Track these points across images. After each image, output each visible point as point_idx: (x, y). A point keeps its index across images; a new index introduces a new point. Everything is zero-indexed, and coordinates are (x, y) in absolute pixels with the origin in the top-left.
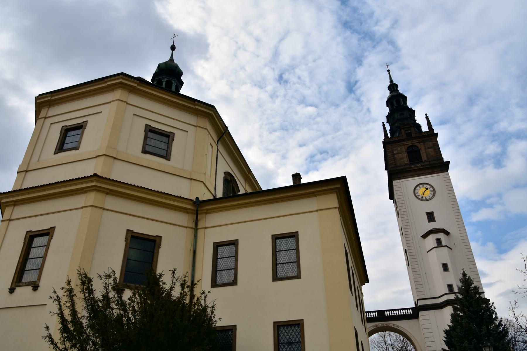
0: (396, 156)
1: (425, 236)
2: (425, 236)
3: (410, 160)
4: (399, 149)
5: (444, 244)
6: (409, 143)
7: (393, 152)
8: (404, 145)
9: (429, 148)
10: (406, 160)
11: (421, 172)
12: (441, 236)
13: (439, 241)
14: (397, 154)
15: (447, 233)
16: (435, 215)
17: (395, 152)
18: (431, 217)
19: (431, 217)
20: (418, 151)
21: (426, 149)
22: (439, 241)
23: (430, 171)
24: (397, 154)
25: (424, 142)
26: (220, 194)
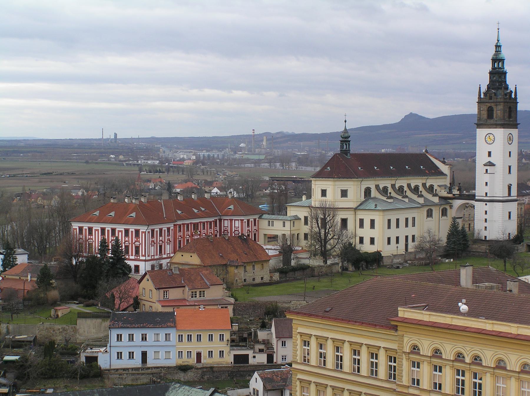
0: (481, 112)
1: (485, 165)
2: (485, 165)
3: (488, 117)
4: (484, 107)
7: (480, 109)
8: (487, 106)
9: (498, 110)
11: (491, 126)
13: (487, 170)
14: (482, 110)
15: (494, 165)
17: (482, 109)
18: (490, 154)
19: (490, 154)
20: (493, 110)
21: (496, 111)
22: (487, 170)
23: (495, 126)
24: (482, 110)
25: (496, 105)
26: (363, 199)
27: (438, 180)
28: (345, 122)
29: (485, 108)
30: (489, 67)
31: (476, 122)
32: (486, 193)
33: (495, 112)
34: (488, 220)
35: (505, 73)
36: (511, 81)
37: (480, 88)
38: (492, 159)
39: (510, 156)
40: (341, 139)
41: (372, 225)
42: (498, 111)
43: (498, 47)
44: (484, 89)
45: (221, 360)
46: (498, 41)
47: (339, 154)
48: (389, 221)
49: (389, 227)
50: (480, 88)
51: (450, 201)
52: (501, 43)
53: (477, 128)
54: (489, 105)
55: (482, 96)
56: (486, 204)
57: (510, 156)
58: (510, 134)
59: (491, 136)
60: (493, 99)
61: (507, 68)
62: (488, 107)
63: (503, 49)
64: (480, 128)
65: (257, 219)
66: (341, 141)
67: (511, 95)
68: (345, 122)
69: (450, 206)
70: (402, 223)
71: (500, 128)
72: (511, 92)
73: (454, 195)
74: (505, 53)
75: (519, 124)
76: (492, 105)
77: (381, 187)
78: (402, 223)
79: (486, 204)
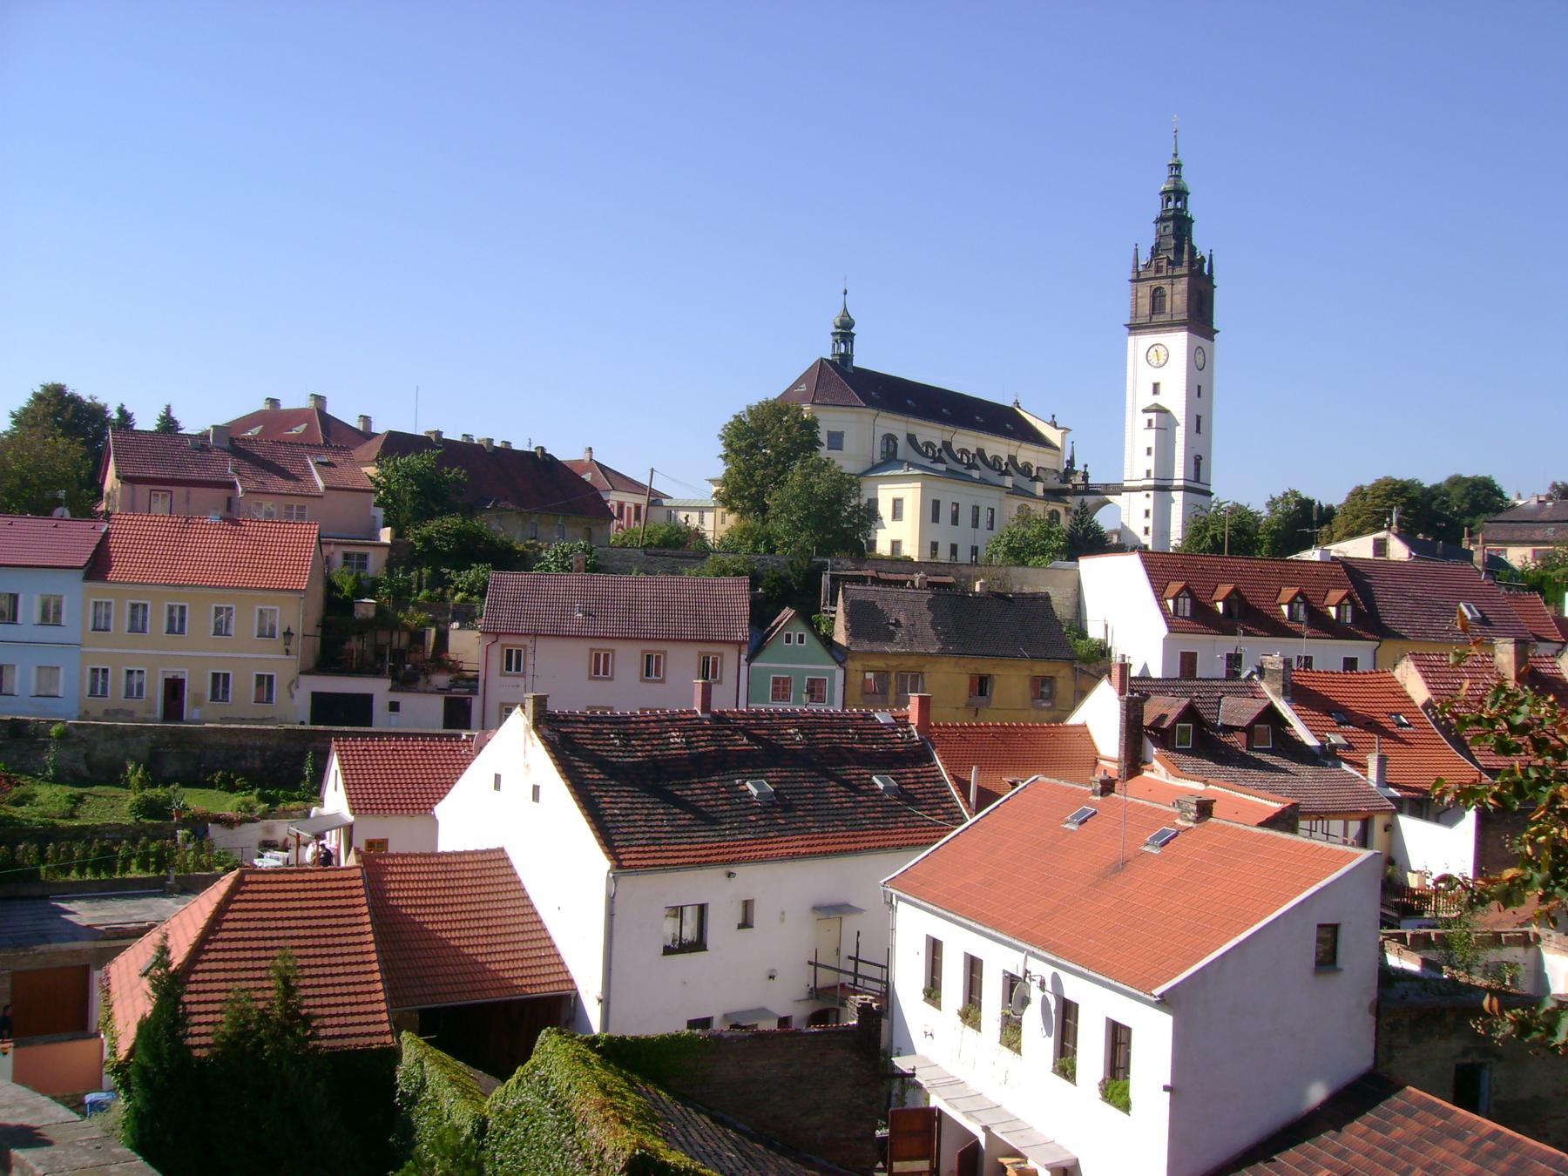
1: (1145, 411)
2: (1145, 411)
5: (1154, 426)
6: (1156, 283)
10: (1145, 307)
12: (1153, 416)
16: (1162, 388)
17: (1139, 295)
18: (1156, 388)
19: (1156, 388)
22: (1150, 422)
26: (878, 459)
27: (1041, 456)
28: (845, 293)
29: (1145, 290)
30: (1155, 208)
32: (1148, 472)
33: (1168, 298)
34: (1151, 530)
35: (1191, 221)
36: (1202, 240)
38: (1162, 400)
39: (1199, 395)
40: (835, 330)
41: (897, 514)
42: (1178, 294)
45: (263, 710)
46: (1175, 155)
47: (827, 360)
48: (936, 504)
49: (936, 518)
51: (1069, 499)
52: (1181, 158)
53: (1130, 334)
54: (1156, 283)
55: (1140, 269)
56: (1148, 496)
57: (1199, 395)
58: (1199, 347)
59: (1161, 349)
60: (1164, 271)
61: (1193, 210)
63: (1184, 171)
64: (1135, 334)
65: (644, 508)
66: (833, 334)
67: (1201, 267)
68: (845, 293)
69: (1066, 508)
70: (965, 517)
71: (1181, 330)
73: (1075, 486)
74: (1188, 180)
75: (1217, 332)
76: (1163, 281)
77: (920, 440)
78: (965, 517)
79: (1148, 496)
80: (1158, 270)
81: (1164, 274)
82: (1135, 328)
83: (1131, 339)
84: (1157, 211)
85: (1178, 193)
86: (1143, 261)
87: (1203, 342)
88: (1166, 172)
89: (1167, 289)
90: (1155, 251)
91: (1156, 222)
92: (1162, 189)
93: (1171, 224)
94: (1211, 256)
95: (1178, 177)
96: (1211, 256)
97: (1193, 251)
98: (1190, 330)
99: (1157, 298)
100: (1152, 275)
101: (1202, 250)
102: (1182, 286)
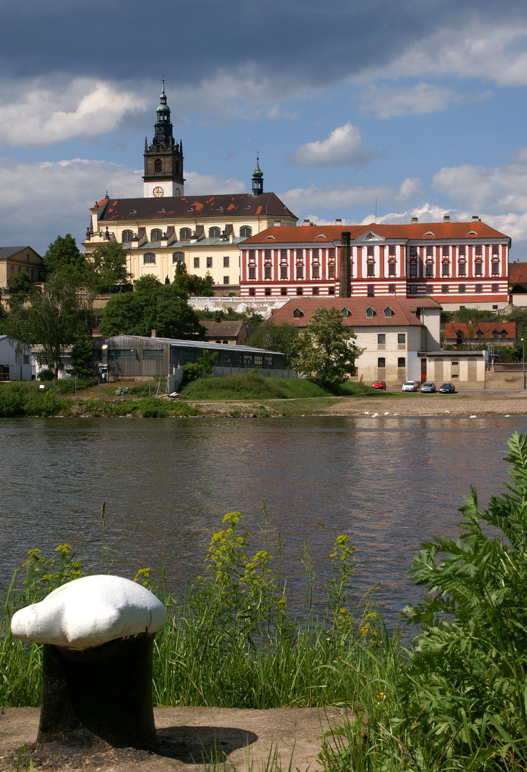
6: (156, 158)
29: (151, 162)
30: (155, 119)
31: (144, 176)
35: (171, 126)
36: (177, 135)
37: (146, 140)
43: (165, 98)
44: (150, 143)
46: (163, 93)
50: (146, 140)
53: (145, 182)
58: (178, 188)
59: (160, 190)
61: (172, 121)
62: (155, 160)
64: (147, 182)
67: (177, 149)
72: (178, 145)
80: (158, 151)
81: (160, 153)
82: (147, 179)
83: (146, 184)
84: (155, 121)
85: (166, 112)
86: (149, 145)
87: (178, 185)
88: (160, 101)
89: (162, 160)
90: (155, 141)
91: (155, 126)
92: (158, 109)
93: (163, 128)
94: (181, 143)
95: (165, 104)
96: (181, 143)
97: (173, 140)
98: (173, 181)
99: (158, 165)
100: (154, 153)
101: (177, 142)
102: (169, 159)
